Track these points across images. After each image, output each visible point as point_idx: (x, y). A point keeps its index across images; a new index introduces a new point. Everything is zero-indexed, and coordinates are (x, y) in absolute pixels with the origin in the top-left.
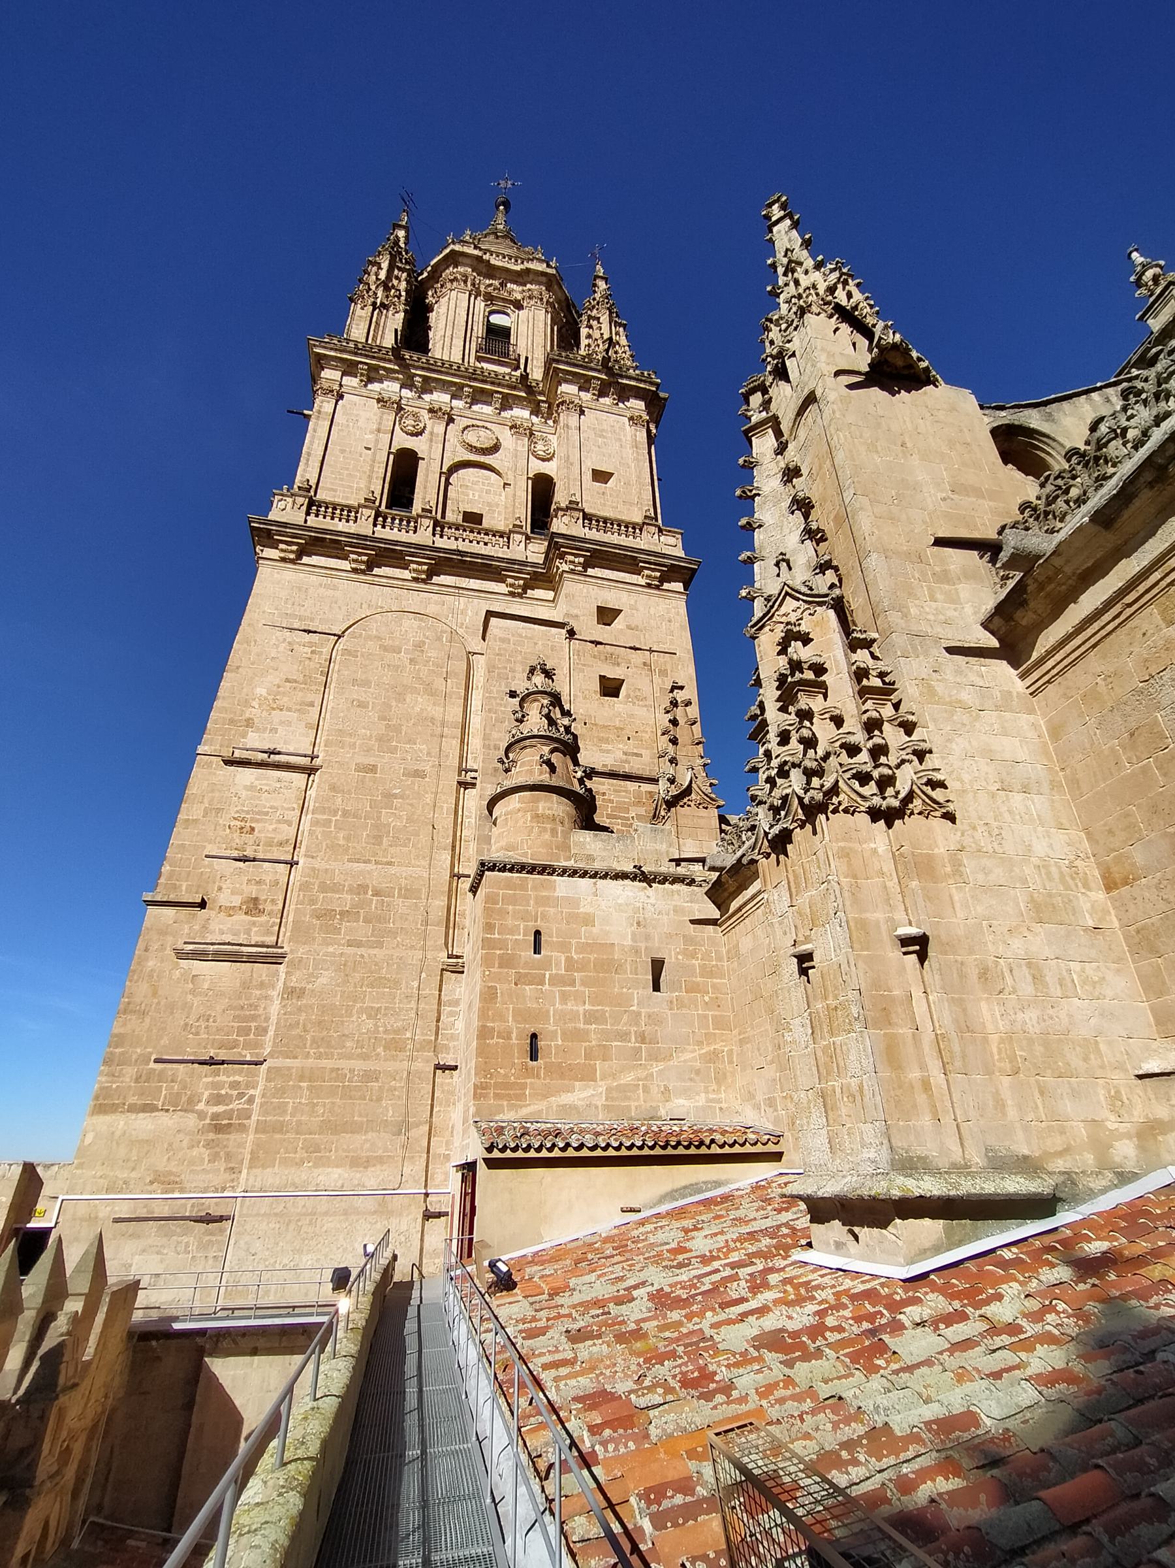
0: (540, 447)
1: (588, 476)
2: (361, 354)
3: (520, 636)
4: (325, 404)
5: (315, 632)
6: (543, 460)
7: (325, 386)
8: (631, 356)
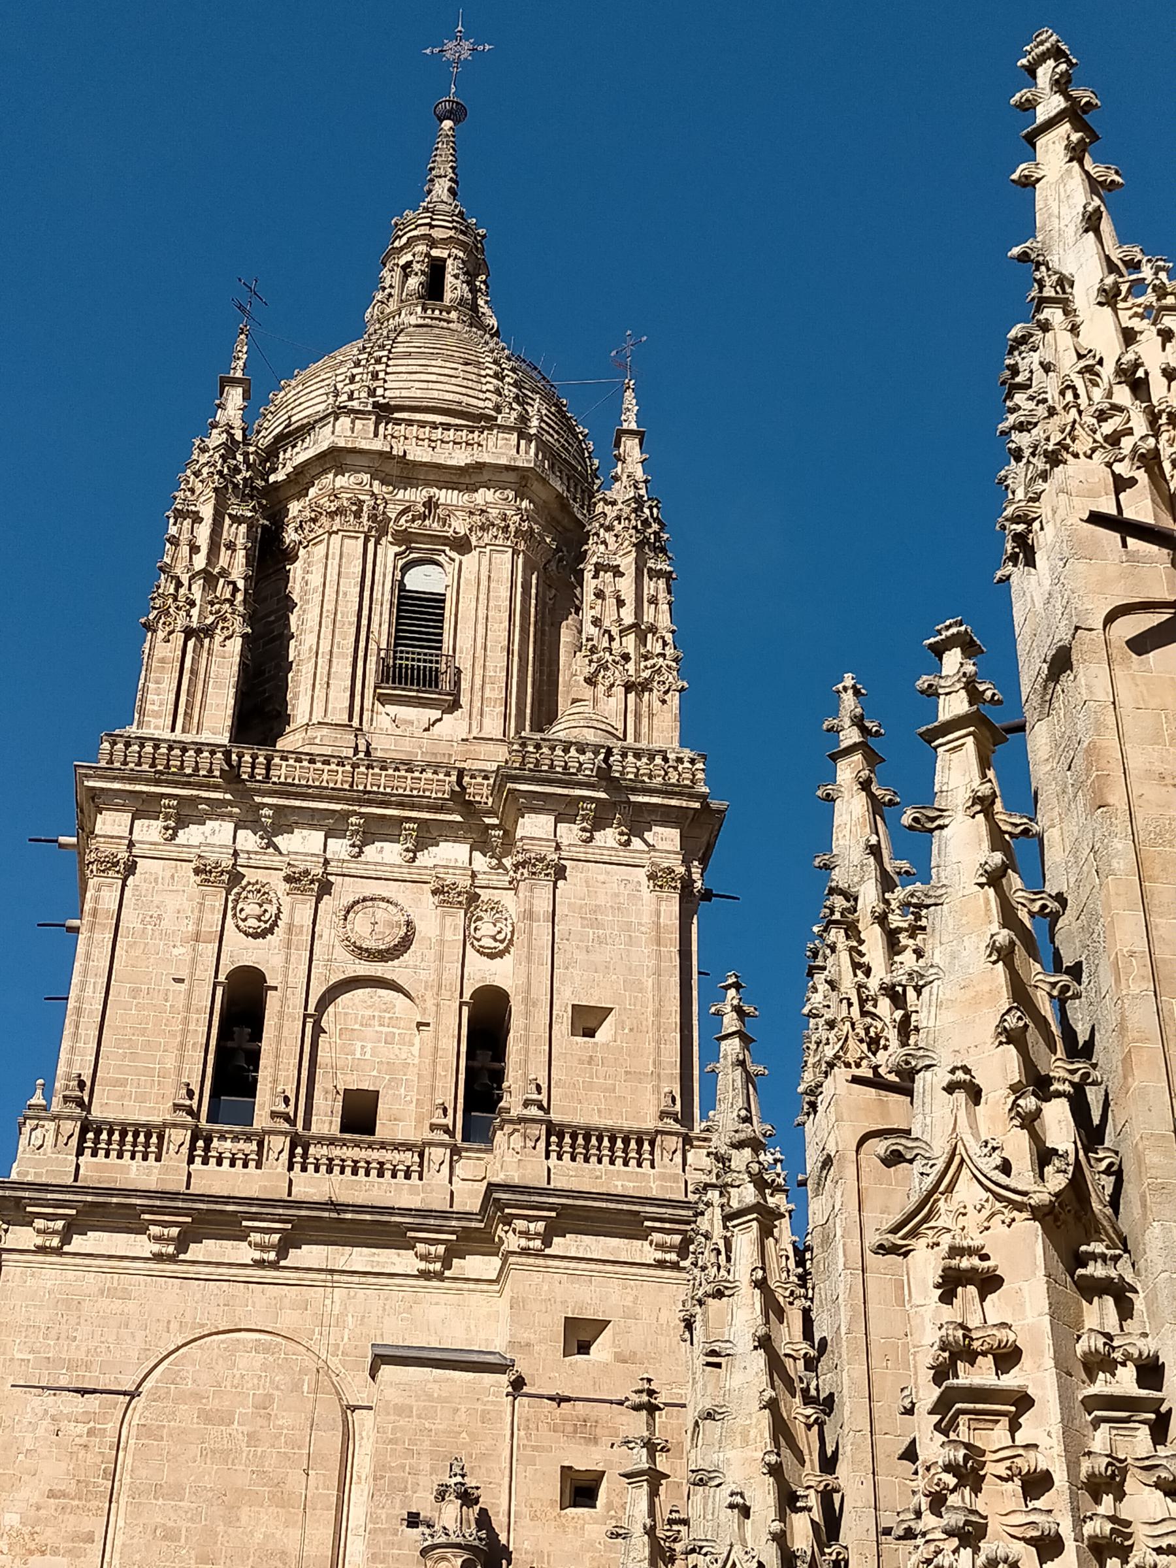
0: (486, 929)
1: (563, 1026)
2: (166, 781)
3: (430, 1398)
4: (105, 893)
5: (94, 1391)
6: (492, 956)
7: (107, 848)
8: (676, 660)
